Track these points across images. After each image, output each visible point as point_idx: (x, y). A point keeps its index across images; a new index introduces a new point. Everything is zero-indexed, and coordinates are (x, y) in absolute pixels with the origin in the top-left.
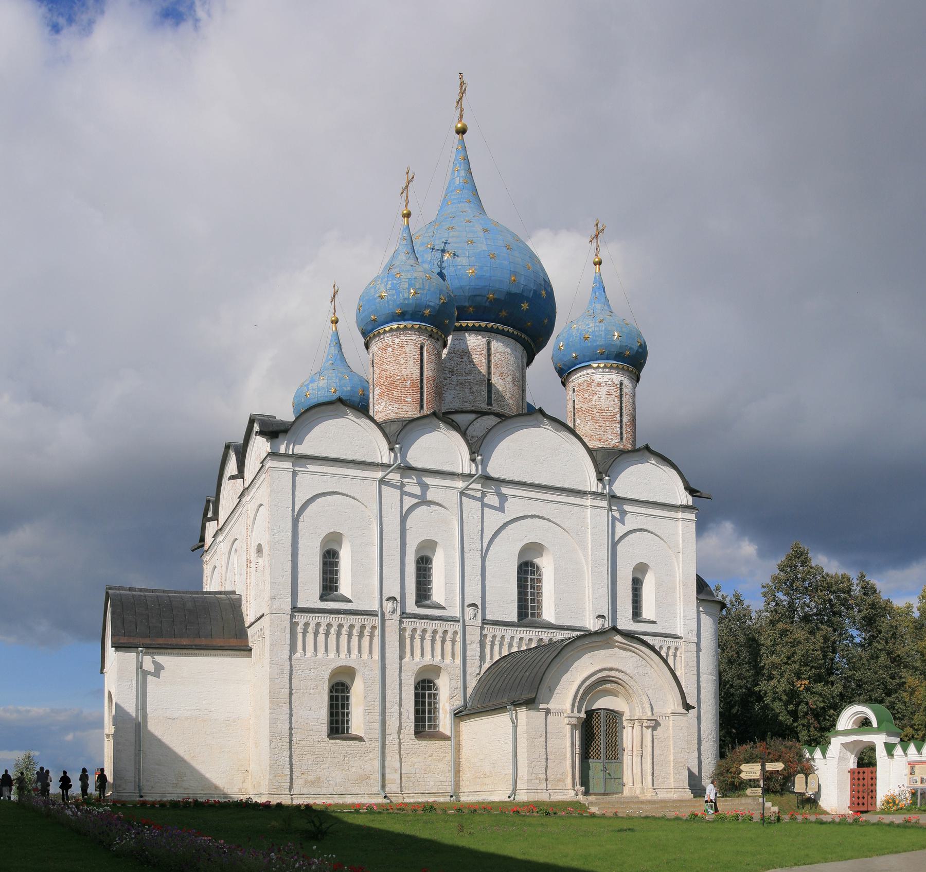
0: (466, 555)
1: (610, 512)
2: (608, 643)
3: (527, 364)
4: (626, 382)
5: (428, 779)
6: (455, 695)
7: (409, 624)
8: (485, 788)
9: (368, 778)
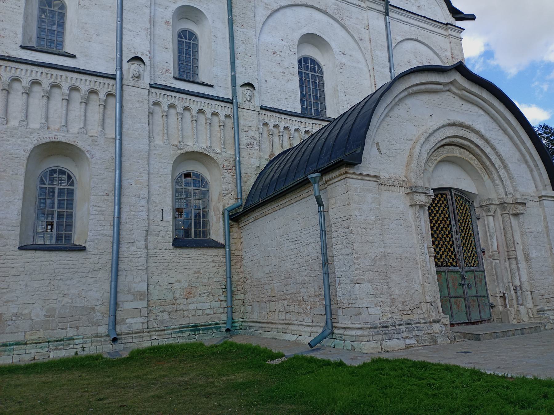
5: (192, 307)
6: (228, 192)
7: (165, 99)
8: (274, 318)
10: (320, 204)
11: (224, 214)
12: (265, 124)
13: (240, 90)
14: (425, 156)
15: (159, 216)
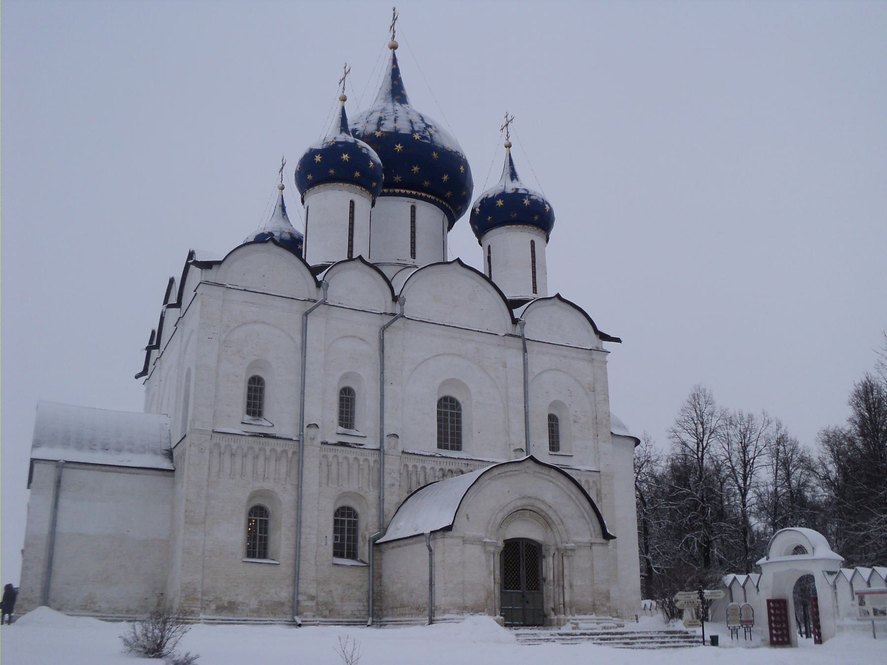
0: (387, 387)
2: (526, 472)
3: (448, 228)
4: (539, 241)
9: (282, 604)
10: (430, 550)
11: (369, 541)
12: (406, 465)
13: (386, 440)
14: (499, 520)
15: (324, 543)
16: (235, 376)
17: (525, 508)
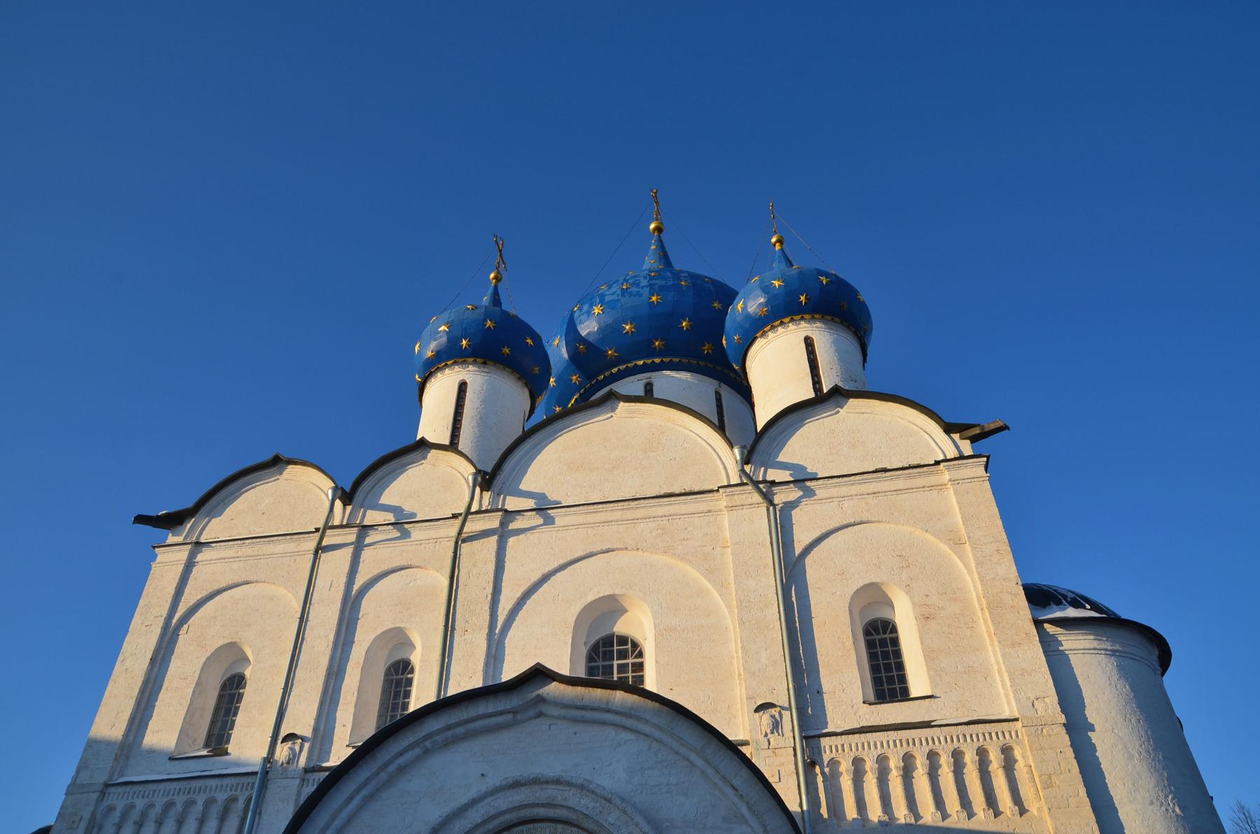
1: (771, 508)
16: (181, 679)
17: (528, 813)
